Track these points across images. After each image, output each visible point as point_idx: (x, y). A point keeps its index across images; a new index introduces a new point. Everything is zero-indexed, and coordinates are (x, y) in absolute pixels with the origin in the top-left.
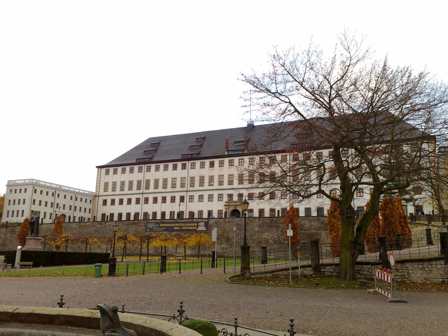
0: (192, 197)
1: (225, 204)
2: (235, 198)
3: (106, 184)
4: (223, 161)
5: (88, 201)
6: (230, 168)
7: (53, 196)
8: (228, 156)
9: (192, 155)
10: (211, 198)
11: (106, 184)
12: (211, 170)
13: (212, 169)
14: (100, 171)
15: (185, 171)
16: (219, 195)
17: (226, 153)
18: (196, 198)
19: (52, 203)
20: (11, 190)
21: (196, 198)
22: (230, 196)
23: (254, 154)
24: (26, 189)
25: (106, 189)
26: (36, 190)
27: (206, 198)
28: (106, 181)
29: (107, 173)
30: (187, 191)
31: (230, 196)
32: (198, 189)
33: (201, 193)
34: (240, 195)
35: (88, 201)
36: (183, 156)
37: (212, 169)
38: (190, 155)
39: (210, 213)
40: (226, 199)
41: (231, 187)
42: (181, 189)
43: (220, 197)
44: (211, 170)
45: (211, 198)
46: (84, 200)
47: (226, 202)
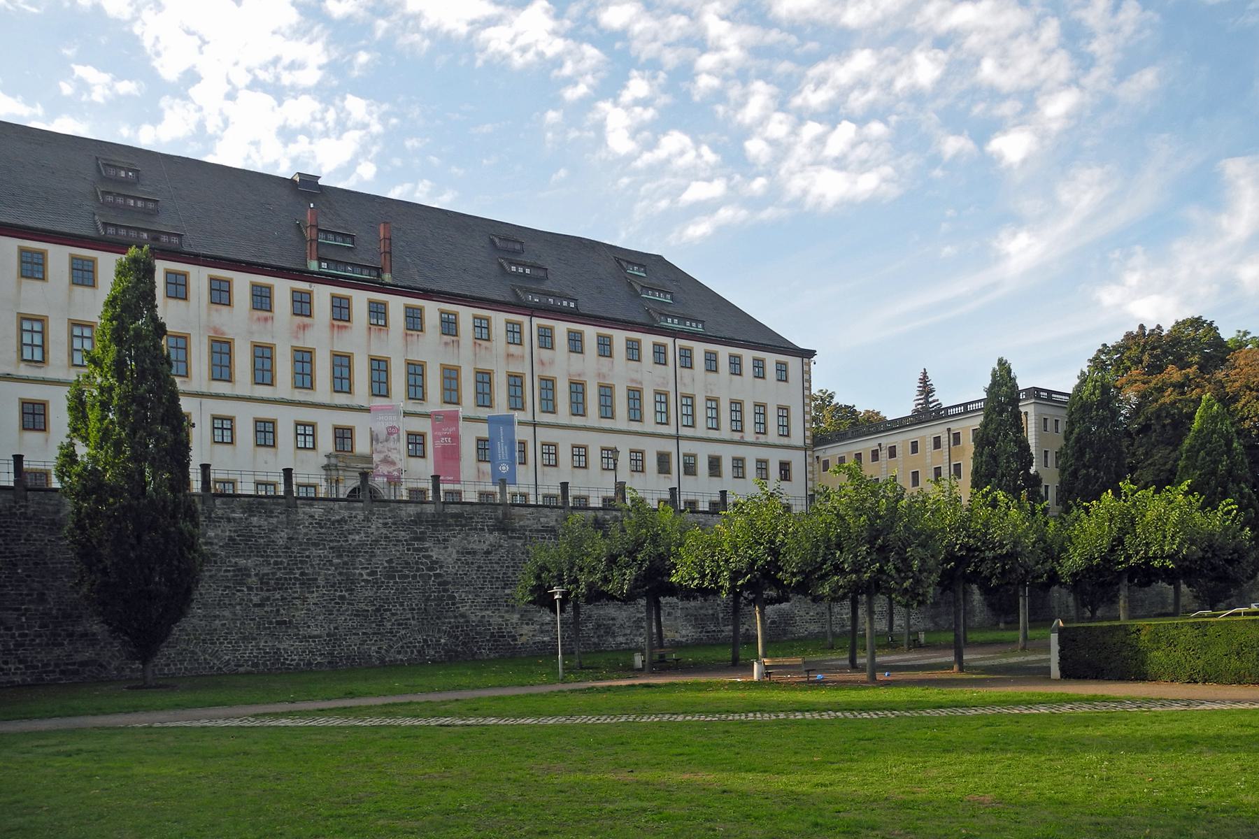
1: (325, 461)
6: (338, 327)
12: (259, 319)
13: (266, 319)
16: (297, 424)
22: (343, 435)
23: (427, 294)
31: (343, 435)
36: (111, 230)
37: (266, 319)
38: (145, 235)
40: (326, 442)
41: (341, 399)
43: (306, 431)
44: (259, 319)
47: (328, 456)
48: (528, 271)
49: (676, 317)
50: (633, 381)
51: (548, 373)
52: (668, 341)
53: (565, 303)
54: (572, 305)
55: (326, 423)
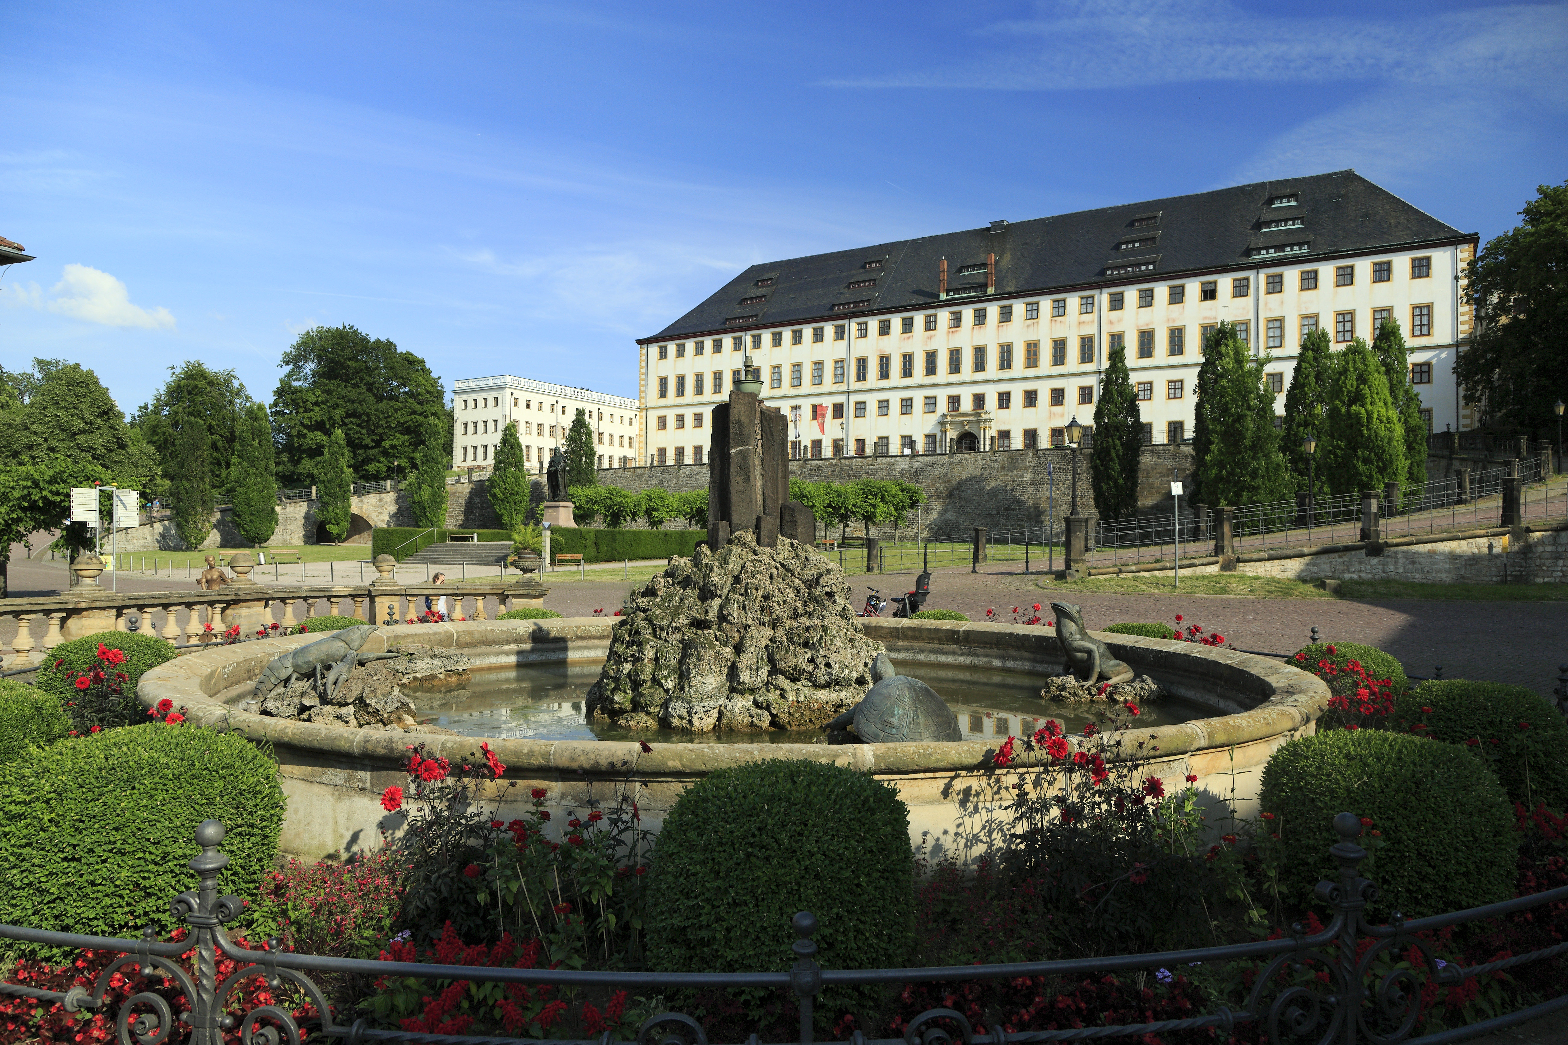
0: (861, 407)
2: (967, 405)
3: (663, 382)
4: (935, 316)
5: (626, 421)
7: (552, 410)
8: (948, 303)
9: (856, 303)
10: (907, 405)
11: (663, 382)
14: (644, 352)
15: (843, 343)
17: (943, 296)
18: (872, 408)
19: (552, 427)
20: (466, 402)
21: (872, 408)
22: (955, 401)
24: (496, 399)
25: (663, 394)
26: (516, 399)
27: (895, 406)
28: (662, 374)
29: (663, 354)
30: (848, 393)
31: (955, 401)
32: (874, 387)
33: (883, 396)
34: (979, 400)
35: (626, 421)
39: (908, 441)
40: (943, 406)
42: (835, 388)
43: (931, 403)
45: (907, 405)
46: (616, 419)
47: (944, 416)
48: (1137, 245)
49: (1271, 247)
50: (1205, 318)
51: (1117, 329)
52: (1251, 275)
53: (1143, 268)
54: (1151, 267)
55: (942, 397)
